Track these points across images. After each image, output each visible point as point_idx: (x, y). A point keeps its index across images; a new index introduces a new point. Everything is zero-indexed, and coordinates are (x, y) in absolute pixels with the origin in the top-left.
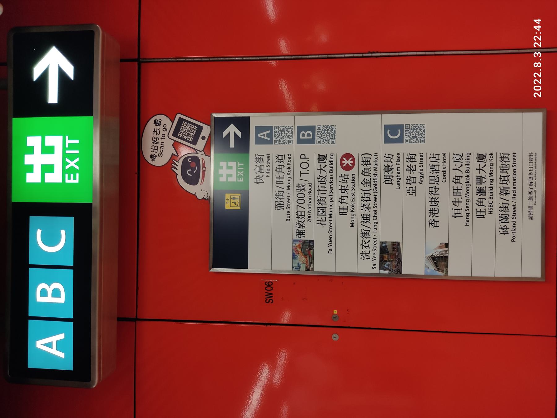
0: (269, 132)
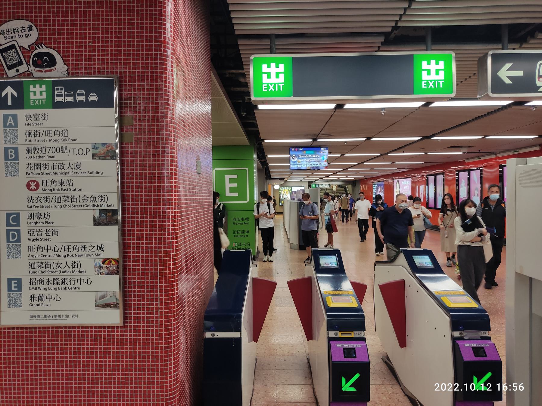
0: (13, 125)
